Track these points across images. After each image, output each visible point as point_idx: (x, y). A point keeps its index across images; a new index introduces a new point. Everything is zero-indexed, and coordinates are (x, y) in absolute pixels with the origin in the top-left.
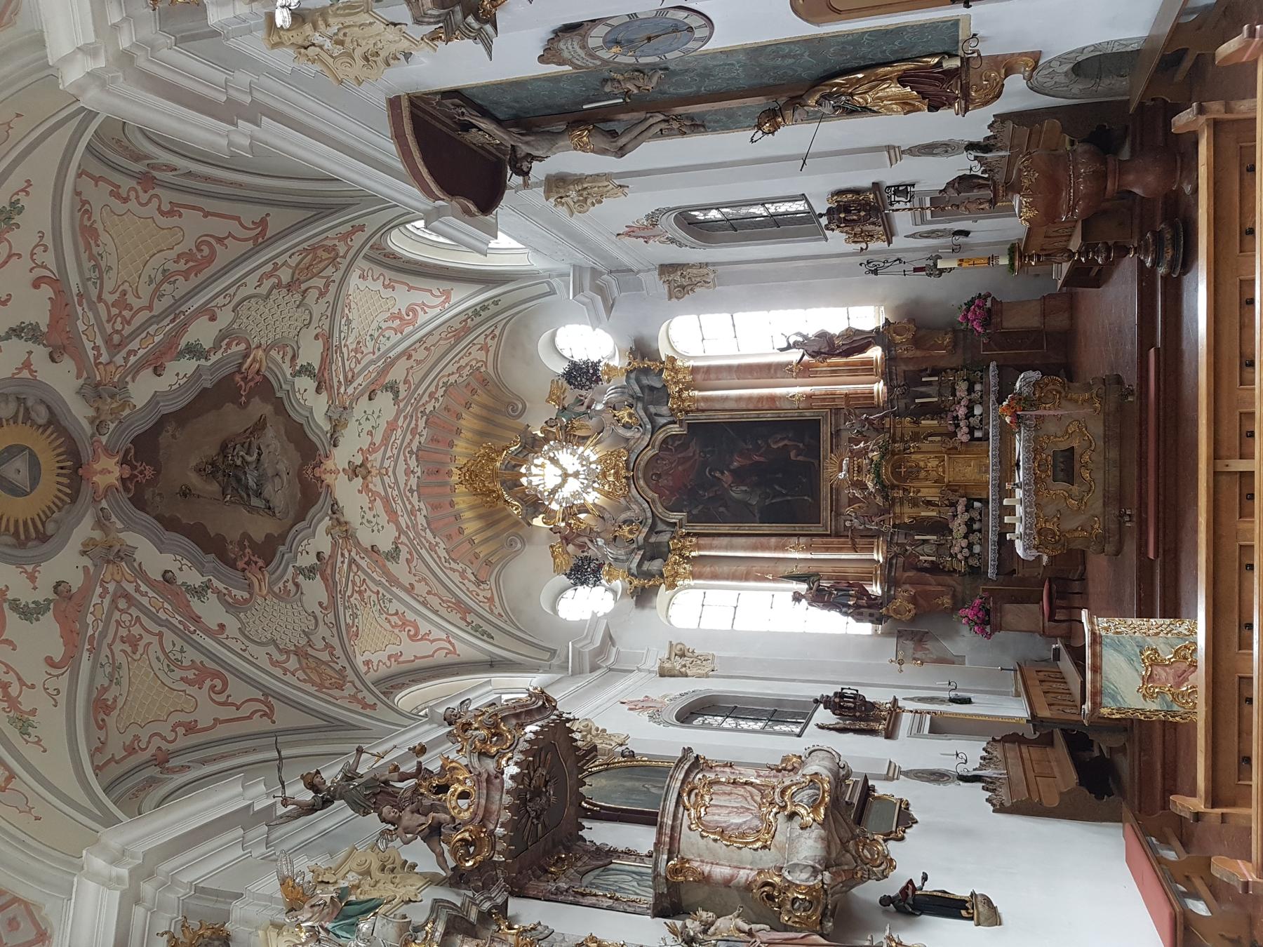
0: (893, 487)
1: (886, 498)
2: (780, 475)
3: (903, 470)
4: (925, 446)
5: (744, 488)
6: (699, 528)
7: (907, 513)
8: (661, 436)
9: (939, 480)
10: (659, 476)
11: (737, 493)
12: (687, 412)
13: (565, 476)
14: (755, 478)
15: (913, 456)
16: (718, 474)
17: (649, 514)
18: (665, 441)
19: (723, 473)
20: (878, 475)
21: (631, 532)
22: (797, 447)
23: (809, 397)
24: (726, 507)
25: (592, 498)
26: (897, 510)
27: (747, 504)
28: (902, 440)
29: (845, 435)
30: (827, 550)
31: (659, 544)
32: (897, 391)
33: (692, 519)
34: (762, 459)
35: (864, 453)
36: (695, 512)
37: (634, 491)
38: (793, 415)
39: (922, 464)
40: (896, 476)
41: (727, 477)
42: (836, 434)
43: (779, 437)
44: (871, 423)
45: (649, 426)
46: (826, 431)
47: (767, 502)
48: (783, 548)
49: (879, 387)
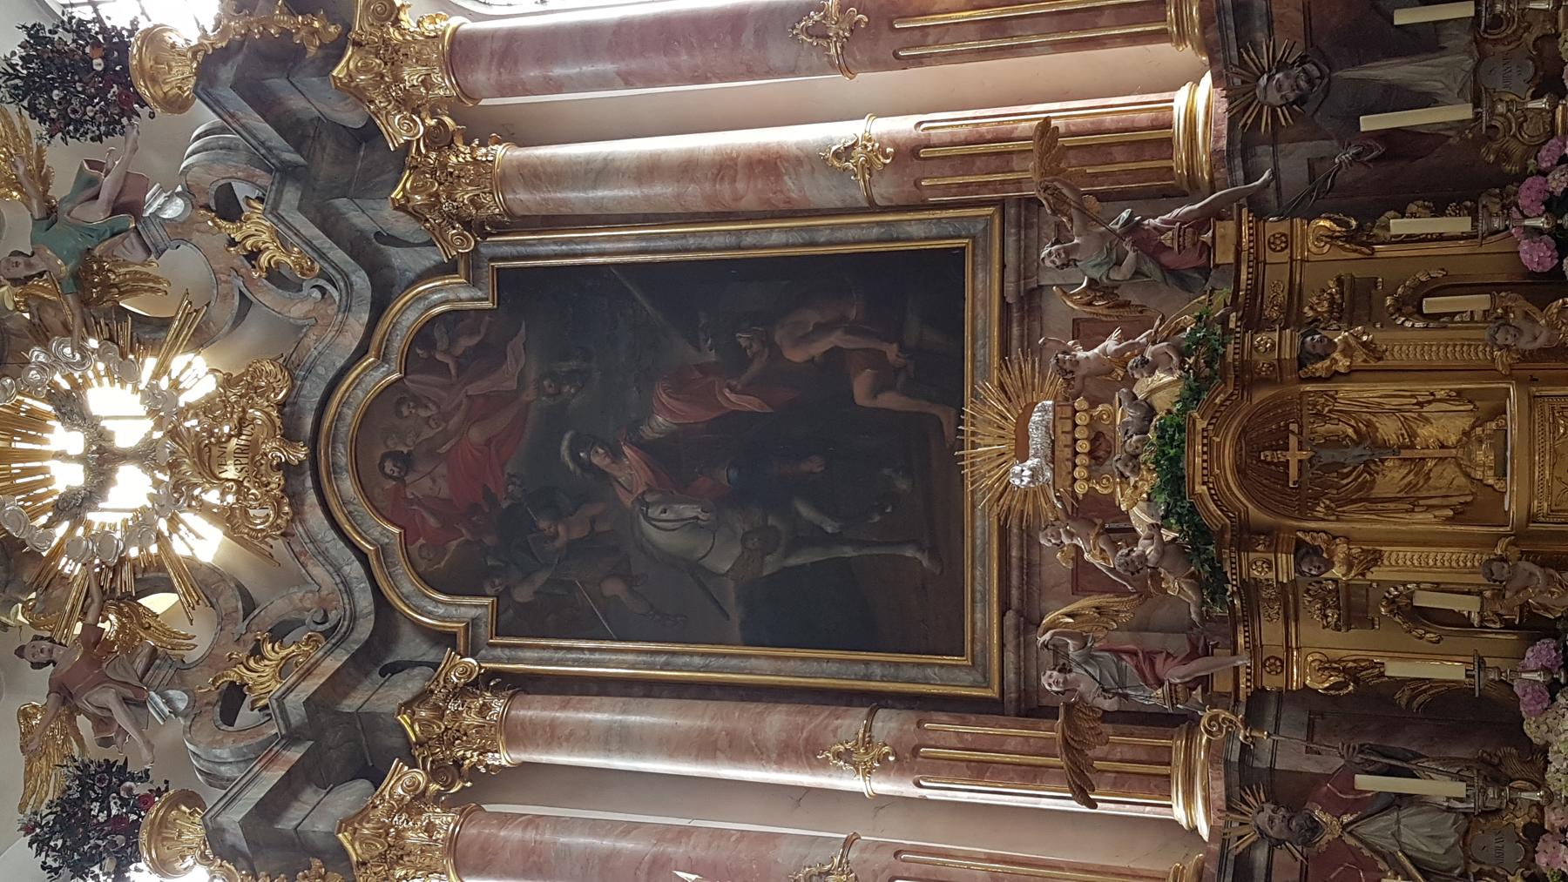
0: (1246, 535)
1: (1211, 584)
2: (814, 465)
3: (1294, 456)
4: (1406, 340)
5: (689, 511)
6: (532, 657)
7: (1313, 654)
8: (406, 317)
9: (1476, 507)
10: (406, 462)
11: (668, 527)
12: (477, 227)
13: (102, 460)
14: (725, 476)
15: (1347, 391)
16: (600, 459)
17: (365, 602)
18: (424, 336)
19: (616, 455)
20: (1174, 481)
21: (282, 671)
22: (876, 360)
23: (909, 154)
24: (629, 579)
25: (203, 542)
26: (1271, 632)
27: (694, 569)
28: (1291, 315)
29: (1064, 307)
30: (980, 772)
31: (367, 722)
32: (1273, 89)
33: (516, 621)
34: (749, 403)
35: (1111, 379)
36: (523, 594)
37: (315, 516)
38: (858, 235)
39: (1388, 429)
40: (1260, 485)
41: (631, 471)
42: (1025, 304)
43: (812, 317)
44: (1148, 244)
45: (361, 280)
46: (984, 293)
47: (771, 565)
48: (807, 752)
49: (1197, 100)
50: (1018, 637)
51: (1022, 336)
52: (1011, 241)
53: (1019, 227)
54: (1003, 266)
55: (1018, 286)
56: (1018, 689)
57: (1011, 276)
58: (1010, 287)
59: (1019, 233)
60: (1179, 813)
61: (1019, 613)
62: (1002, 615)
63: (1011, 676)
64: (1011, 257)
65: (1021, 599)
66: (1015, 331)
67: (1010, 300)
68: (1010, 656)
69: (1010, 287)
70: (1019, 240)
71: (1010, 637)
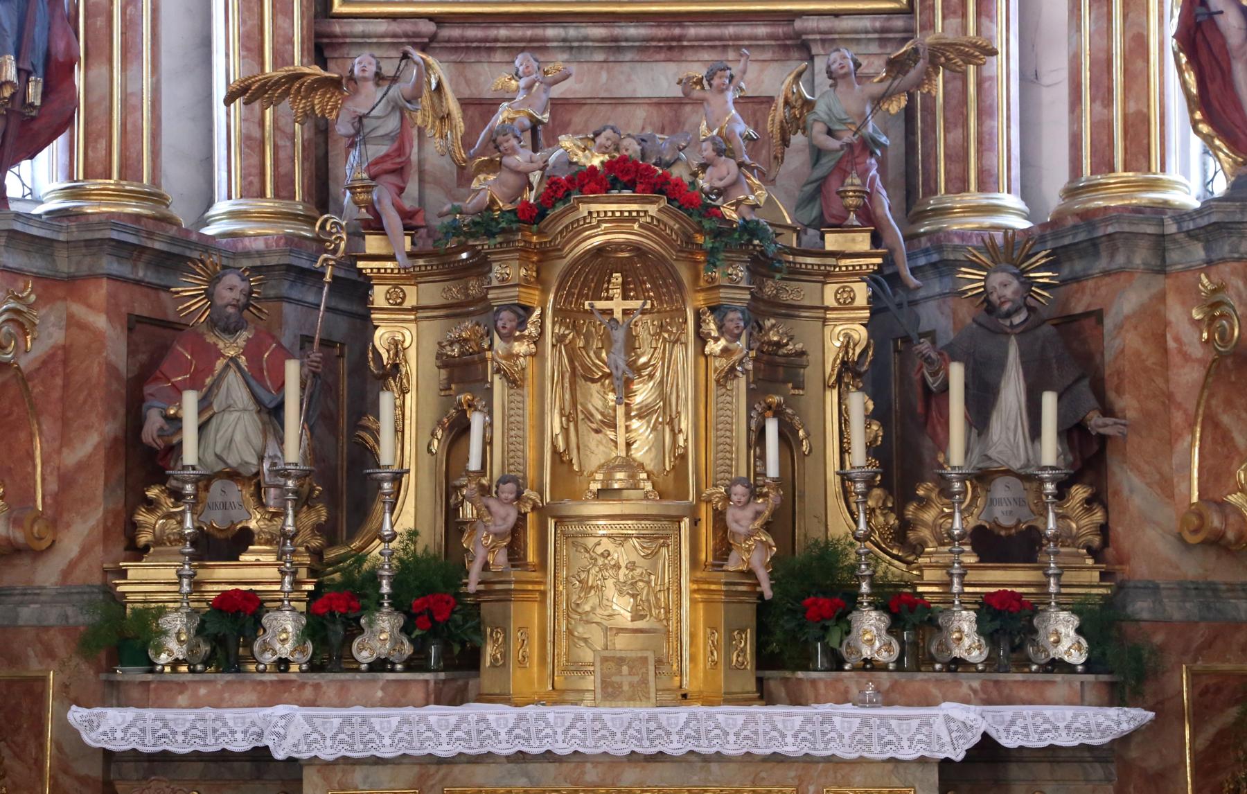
3: (617, 305)
50: (406, 35)
51: (756, 38)
52: (866, 22)
53: (883, 30)
54: (836, 14)
55: (813, 32)
56: (345, 36)
57: (825, 24)
58: (812, 23)
59: (875, 31)
60: (222, 206)
61: (433, 38)
62: (431, 17)
63: (359, 27)
64: (846, 23)
65: (449, 41)
66: (762, 30)
67: (798, 24)
68: (382, 27)
69: (812, 23)
70: (867, 32)
71: (407, 26)
